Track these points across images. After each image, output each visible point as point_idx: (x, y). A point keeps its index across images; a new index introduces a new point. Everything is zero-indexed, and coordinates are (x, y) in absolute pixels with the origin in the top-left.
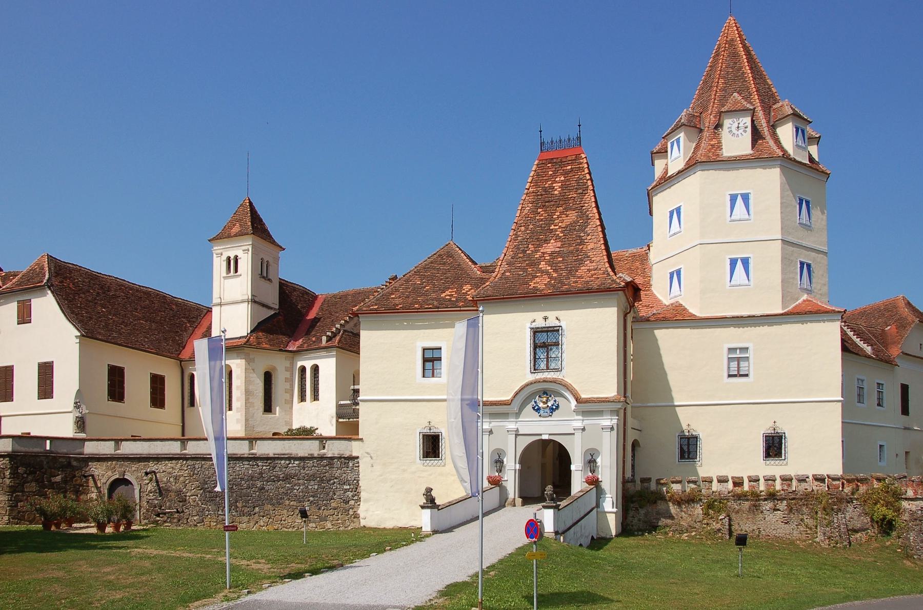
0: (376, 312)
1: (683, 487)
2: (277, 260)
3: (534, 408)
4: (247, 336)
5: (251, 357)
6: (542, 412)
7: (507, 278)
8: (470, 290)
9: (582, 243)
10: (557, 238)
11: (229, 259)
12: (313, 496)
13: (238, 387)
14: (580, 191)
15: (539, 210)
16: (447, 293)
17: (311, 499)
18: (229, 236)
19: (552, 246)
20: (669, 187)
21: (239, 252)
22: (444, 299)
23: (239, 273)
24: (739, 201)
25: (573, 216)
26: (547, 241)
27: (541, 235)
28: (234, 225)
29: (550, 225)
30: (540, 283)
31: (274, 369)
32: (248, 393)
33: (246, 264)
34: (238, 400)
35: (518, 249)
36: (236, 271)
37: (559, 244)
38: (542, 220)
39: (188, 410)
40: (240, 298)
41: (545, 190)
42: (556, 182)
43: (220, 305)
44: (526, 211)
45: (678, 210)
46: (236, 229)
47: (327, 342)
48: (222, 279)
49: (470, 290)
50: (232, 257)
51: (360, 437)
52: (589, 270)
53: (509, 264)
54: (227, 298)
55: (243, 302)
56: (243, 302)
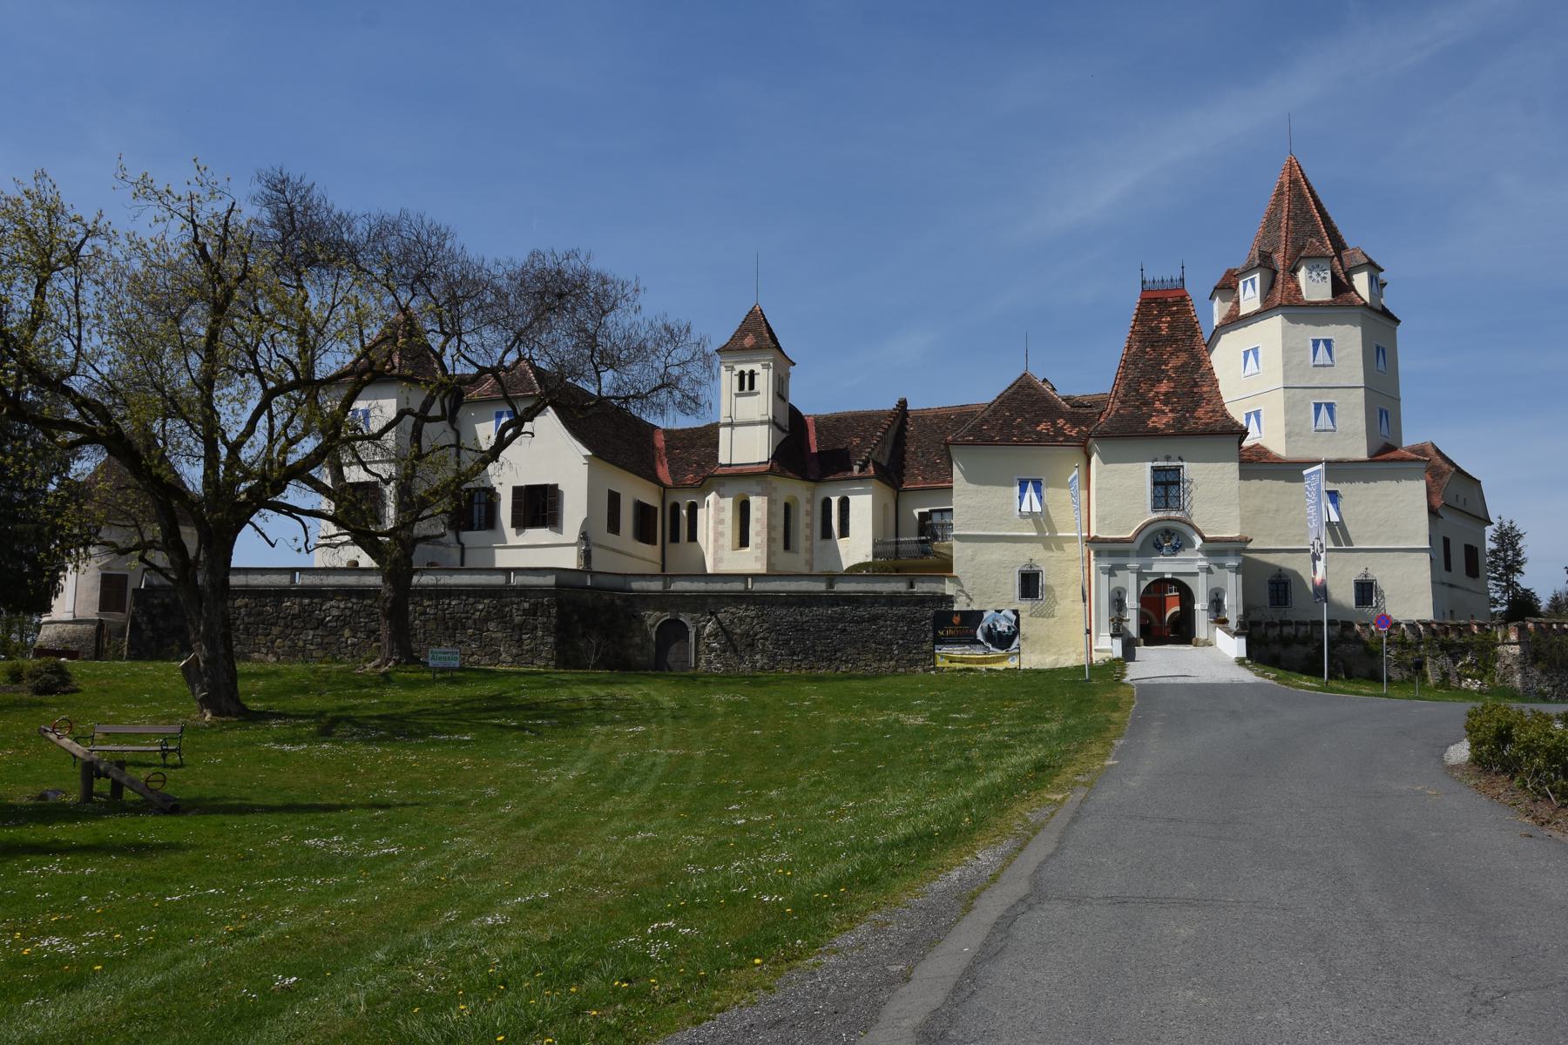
0: (972, 444)
1: (1297, 630)
2: (788, 375)
3: (1155, 546)
4: (767, 462)
5: (774, 485)
6: (1164, 550)
7: (1122, 415)
8: (1065, 424)
9: (1196, 385)
10: (1170, 379)
11: (742, 374)
12: (902, 639)
13: (757, 520)
14: (1189, 333)
15: (1148, 349)
16: (1042, 426)
17: (901, 642)
18: (744, 349)
19: (1164, 387)
20: (1246, 326)
21: (757, 367)
22: (1040, 432)
23: (756, 389)
24: (1322, 346)
25: (1184, 357)
26: (1160, 381)
27: (1154, 373)
28: (746, 336)
29: (1161, 365)
30: (1159, 422)
31: (795, 500)
32: (771, 528)
33: (764, 379)
34: (757, 534)
35: (1130, 387)
36: (752, 386)
37: (1172, 385)
38: (1151, 360)
39: (669, 546)
40: (758, 418)
41: (1152, 329)
42: (1163, 322)
43: (731, 425)
44: (1133, 350)
45: (1255, 351)
46: (749, 341)
47: (860, 471)
48: (734, 396)
49: (1065, 424)
50: (747, 372)
51: (954, 573)
52: (1207, 412)
53: (1121, 402)
54: (740, 416)
55: (762, 423)
56: (762, 423)
